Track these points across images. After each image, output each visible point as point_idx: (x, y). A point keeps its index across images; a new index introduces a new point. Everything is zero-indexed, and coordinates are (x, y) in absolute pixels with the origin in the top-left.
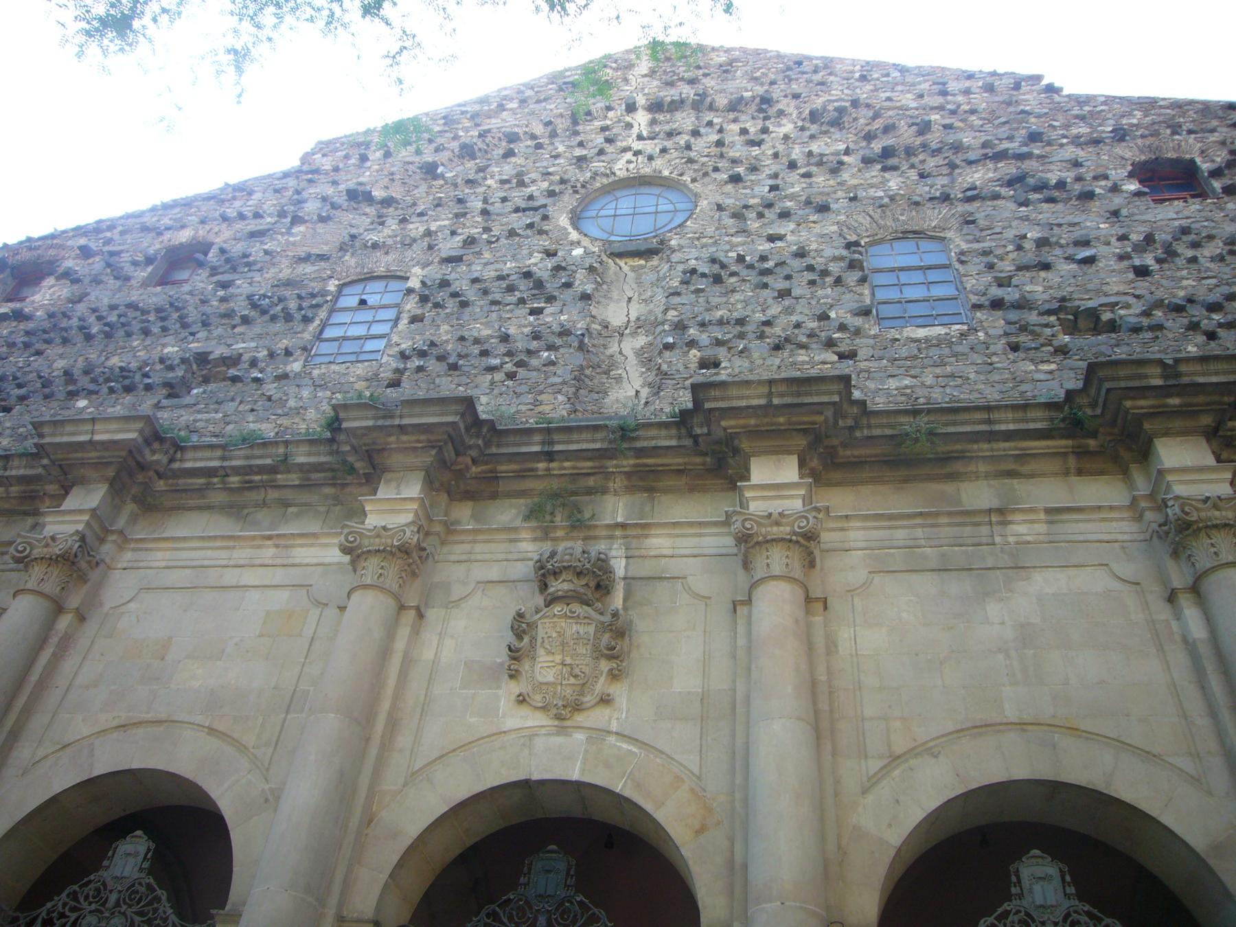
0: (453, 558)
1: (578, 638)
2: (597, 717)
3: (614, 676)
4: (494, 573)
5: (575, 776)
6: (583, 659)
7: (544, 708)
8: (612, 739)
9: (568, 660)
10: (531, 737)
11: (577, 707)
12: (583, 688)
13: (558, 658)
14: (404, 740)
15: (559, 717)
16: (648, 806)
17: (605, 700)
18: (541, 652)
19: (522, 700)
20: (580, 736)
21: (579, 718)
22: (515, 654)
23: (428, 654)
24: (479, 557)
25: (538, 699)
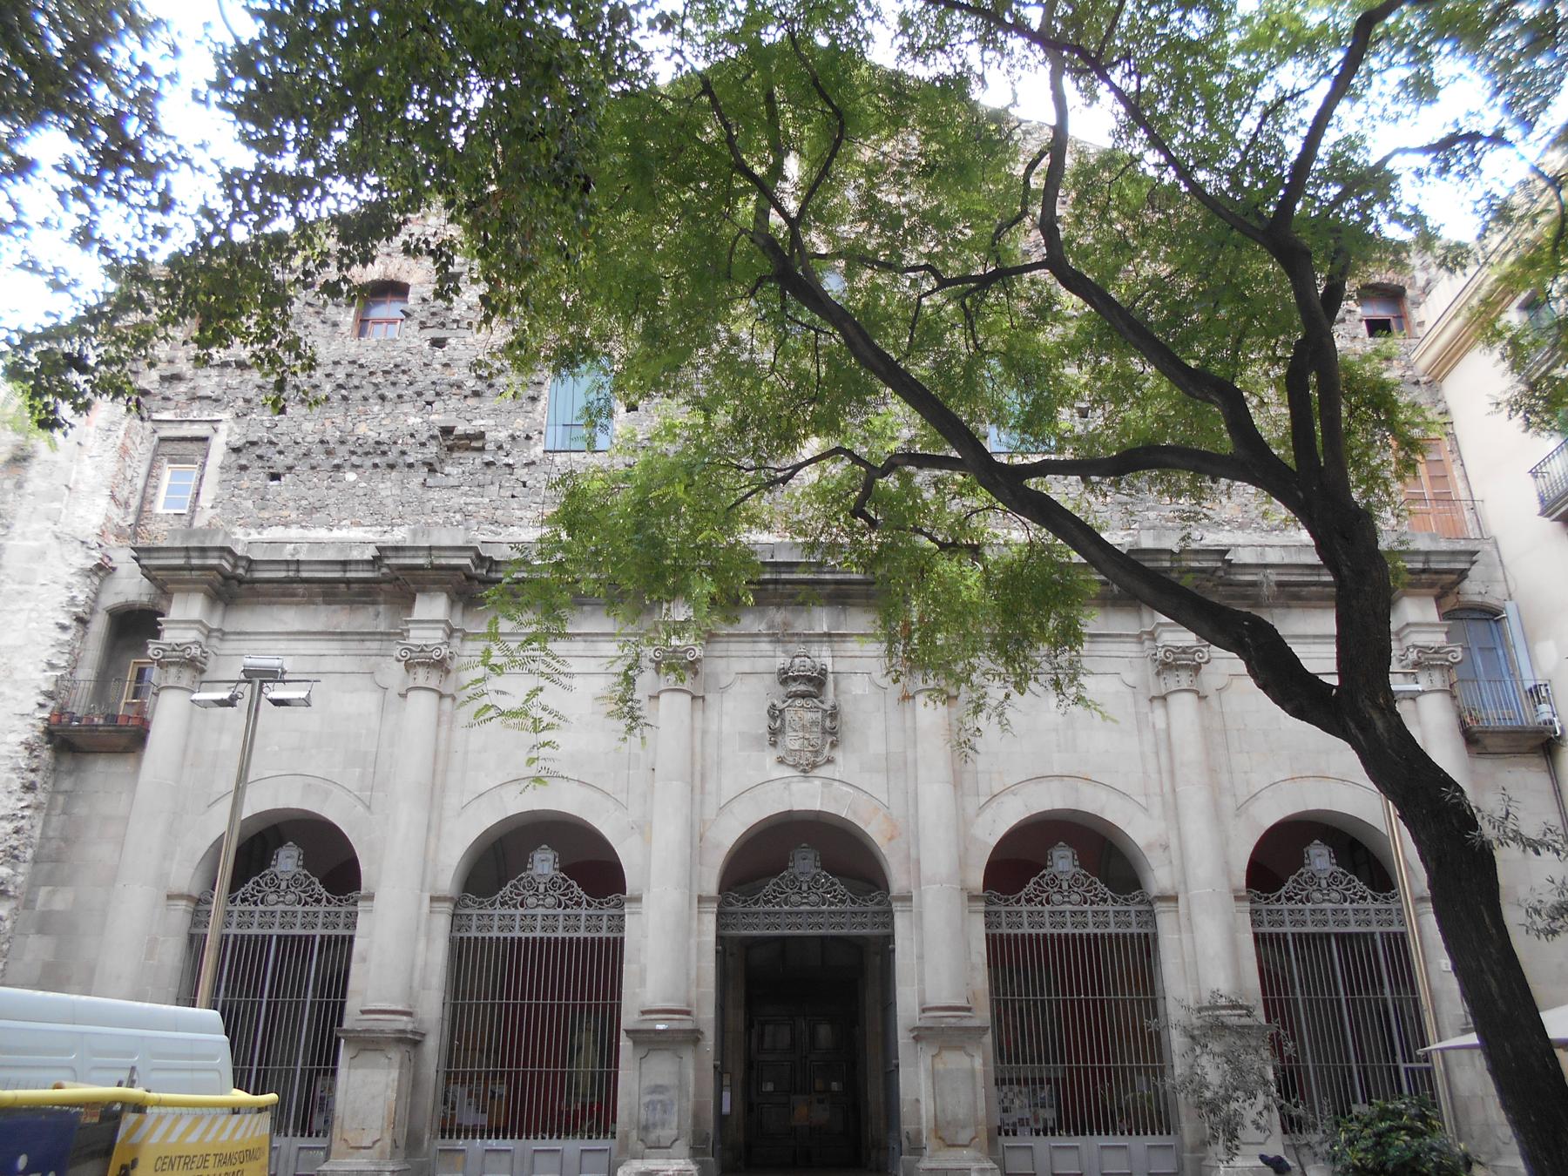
0: (716, 654)
1: (813, 723)
2: (825, 771)
3: (833, 745)
4: (746, 666)
5: (818, 808)
6: (815, 736)
7: (794, 766)
8: (836, 784)
9: (807, 736)
10: (789, 784)
11: (815, 766)
12: (816, 753)
13: (801, 734)
14: (711, 786)
15: (804, 771)
16: (862, 826)
17: (830, 761)
18: (788, 729)
19: (781, 761)
20: (817, 782)
21: (817, 772)
22: (774, 732)
23: (714, 727)
24: (734, 654)
25: (790, 760)
